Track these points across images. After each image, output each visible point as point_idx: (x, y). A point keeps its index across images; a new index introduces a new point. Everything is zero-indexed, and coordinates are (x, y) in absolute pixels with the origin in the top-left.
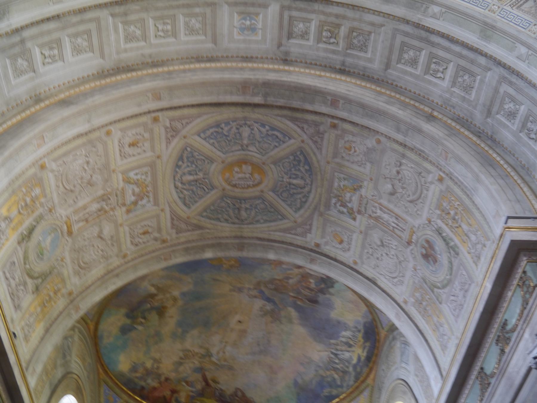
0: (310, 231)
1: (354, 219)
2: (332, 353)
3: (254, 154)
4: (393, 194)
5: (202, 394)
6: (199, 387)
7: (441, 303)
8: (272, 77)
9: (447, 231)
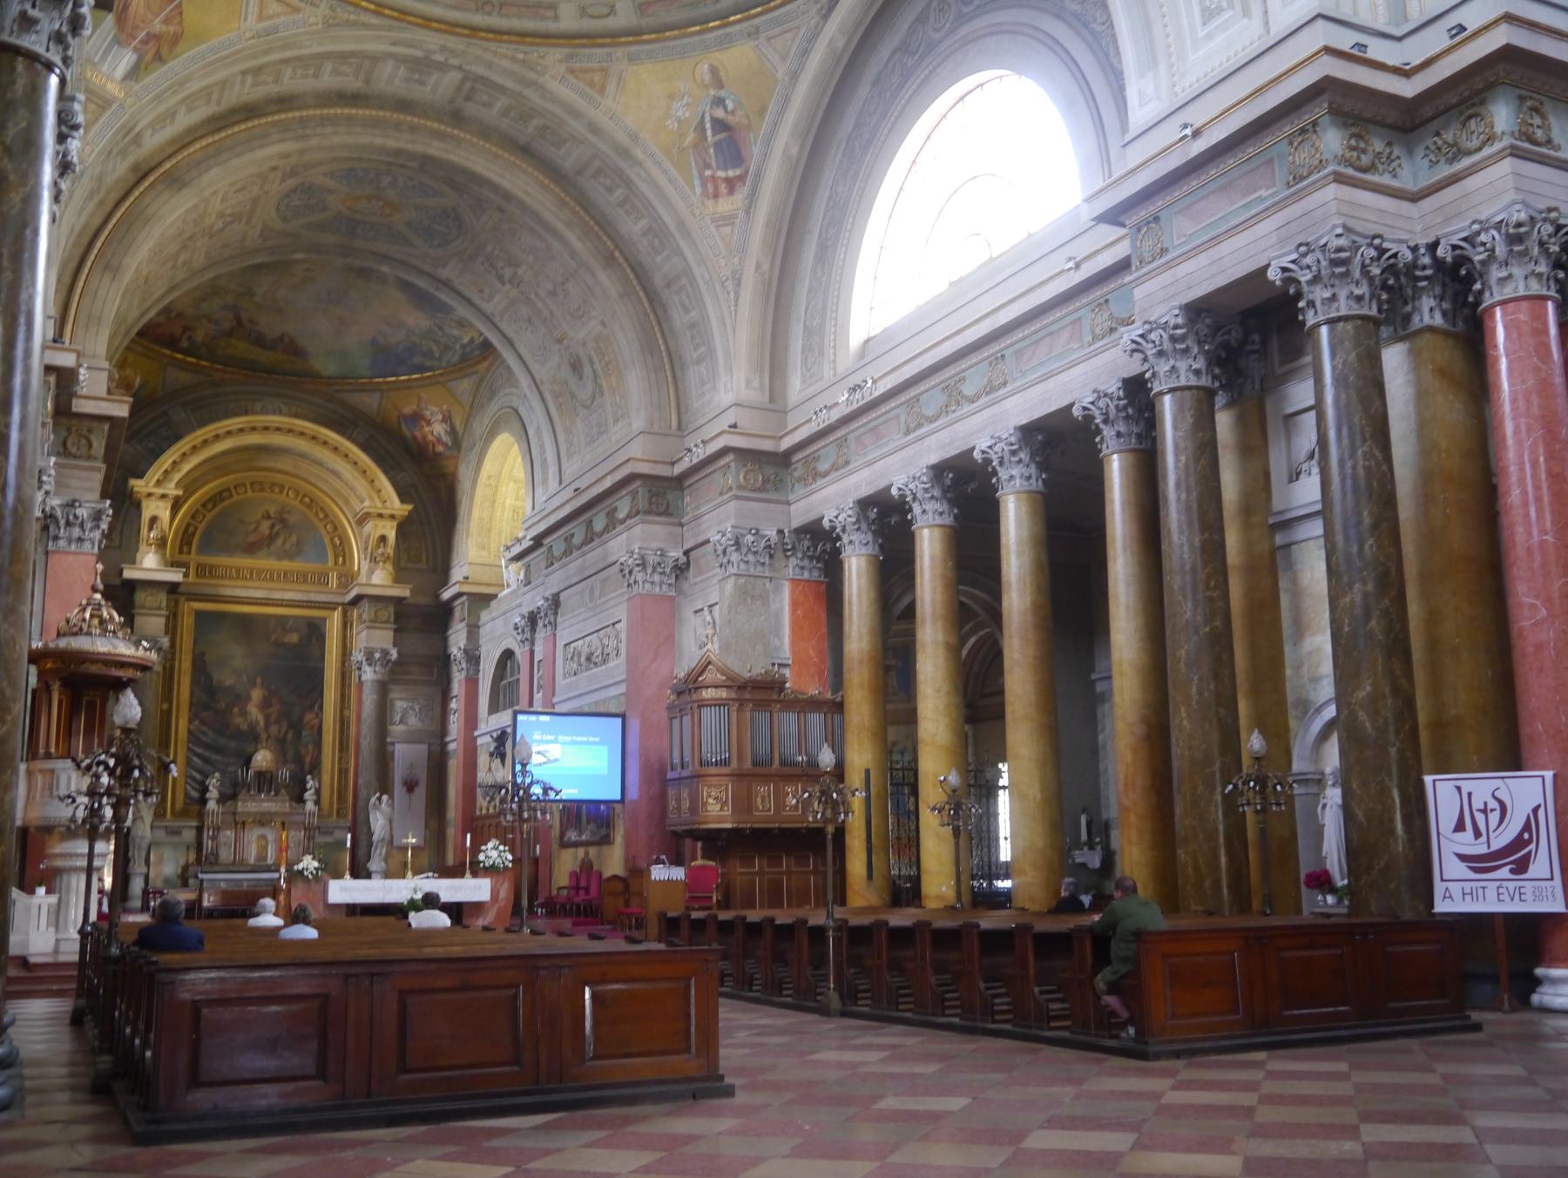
0: (444, 266)
1: (504, 284)
2: (435, 324)
4: (553, 293)
5: (230, 334)
6: (227, 325)
7: (577, 415)
8: (435, 149)
9: (597, 366)
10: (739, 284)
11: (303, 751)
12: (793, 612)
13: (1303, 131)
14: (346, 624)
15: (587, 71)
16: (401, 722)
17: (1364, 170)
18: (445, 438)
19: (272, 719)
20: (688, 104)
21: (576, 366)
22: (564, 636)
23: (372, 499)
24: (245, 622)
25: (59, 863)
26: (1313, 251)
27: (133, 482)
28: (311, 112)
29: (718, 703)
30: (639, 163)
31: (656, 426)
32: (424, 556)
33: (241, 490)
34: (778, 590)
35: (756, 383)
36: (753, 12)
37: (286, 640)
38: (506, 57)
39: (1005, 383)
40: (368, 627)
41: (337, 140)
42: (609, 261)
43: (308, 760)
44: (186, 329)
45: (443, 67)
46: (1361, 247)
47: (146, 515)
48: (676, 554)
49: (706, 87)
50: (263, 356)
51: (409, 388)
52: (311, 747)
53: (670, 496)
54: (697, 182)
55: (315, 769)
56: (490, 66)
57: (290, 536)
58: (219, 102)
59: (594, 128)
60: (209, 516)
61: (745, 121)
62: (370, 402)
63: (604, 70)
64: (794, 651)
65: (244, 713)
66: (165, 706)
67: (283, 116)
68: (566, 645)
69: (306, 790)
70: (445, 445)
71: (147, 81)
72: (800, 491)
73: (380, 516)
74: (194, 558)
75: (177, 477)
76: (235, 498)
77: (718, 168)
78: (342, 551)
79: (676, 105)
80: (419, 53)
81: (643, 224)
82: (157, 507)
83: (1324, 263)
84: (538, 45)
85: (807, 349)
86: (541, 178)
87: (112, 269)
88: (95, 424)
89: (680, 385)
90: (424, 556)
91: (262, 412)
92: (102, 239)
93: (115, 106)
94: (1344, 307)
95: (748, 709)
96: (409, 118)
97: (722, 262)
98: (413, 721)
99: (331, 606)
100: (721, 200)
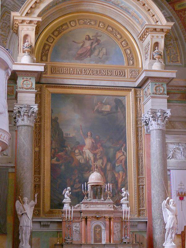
11: (116, 176)
14: (137, 99)
16: (172, 158)
27: (13, 14)
32: (179, 57)
40: (152, 97)
43: (120, 181)
47: (22, 34)
52: (121, 173)
57: (102, 50)
65: (82, 153)
69: (123, 197)
75: (38, 11)
78: (132, 57)
82: (28, 29)
90: (179, 57)
98: (179, 156)
99: (128, 89)
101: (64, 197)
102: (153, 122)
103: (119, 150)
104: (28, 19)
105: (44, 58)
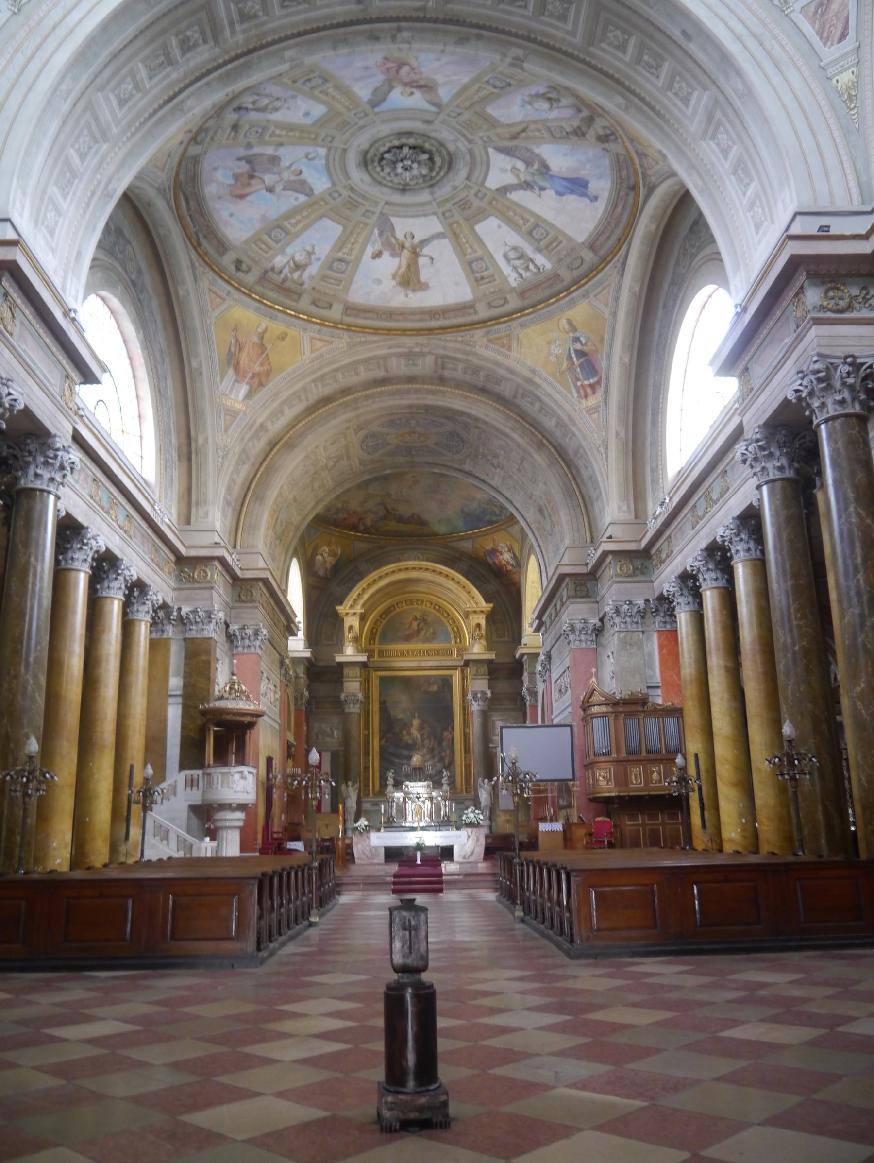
0: (465, 463)
3: (419, 429)
4: (519, 470)
5: (384, 518)
6: (382, 514)
8: (430, 400)
10: (607, 448)
12: (660, 652)
13: (797, 294)
14: (463, 678)
15: (499, 338)
17: (842, 311)
18: (512, 561)
19: (425, 736)
20: (559, 345)
21: (541, 511)
22: (554, 676)
23: (470, 602)
24: (407, 683)
25: (219, 824)
26: (807, 375)
28: (360, 394)
29: (603, 715)
30: (538, 386)
31: (577, 543)
33: (400, 606)
34: (649, 638)
35: (625, 508)
36: (582, 282)
37: (430, 689)
38: (452, 341)
39: (728, 488)
41: (375, 406)
42: (540, 446)
44: (360, 519)
45: (422, 354)
46: (838, 366)
47: (347, 625)
48: (594, 621)
49: (567, 333)
50: (404, 528)
51: (487, 534)
52: (448, 752)
53: (589, 585)
54: (574, 390)
55: (450, 766)
56: (445, 348)
58: (307, 399)
59: (511, 371)
60: (384, 622)
61: (593, 348)
62: (467, 546)
63: (509, 336)
64: (663, 678)
65: (409, 734)
66: (366, 732)
67: (345, 399)
68: (556, 682)
70: (512, 565)
71: (256, 398)
72: (656, 572)
73: (475, 612)
74: (376, 647)
75: (361, 602)
76: (398, 610)
77: (584, 379)
78: (459, 634)
79: (553, 347)
80: (406, 350)
81: (554, 420)
83: (815, 382)
84: (469, 330)
85: (653, 481)
86: (494, 404)
87: (260, 498)
88: (255, 583)
89: (591, 515)
91: (408, 560)
92: (254, 483)
93: (241, 415)
94: (832, 410)
95: (622, 718)
96: (414, 386)
97: (596, 436)
99: (454, 668)
100: (589, 398)
101: (387, 779)
102: (474, 703)
103: (445, 729)
104: (352, 611)
105: (372, 642)
